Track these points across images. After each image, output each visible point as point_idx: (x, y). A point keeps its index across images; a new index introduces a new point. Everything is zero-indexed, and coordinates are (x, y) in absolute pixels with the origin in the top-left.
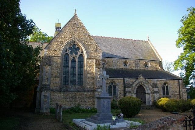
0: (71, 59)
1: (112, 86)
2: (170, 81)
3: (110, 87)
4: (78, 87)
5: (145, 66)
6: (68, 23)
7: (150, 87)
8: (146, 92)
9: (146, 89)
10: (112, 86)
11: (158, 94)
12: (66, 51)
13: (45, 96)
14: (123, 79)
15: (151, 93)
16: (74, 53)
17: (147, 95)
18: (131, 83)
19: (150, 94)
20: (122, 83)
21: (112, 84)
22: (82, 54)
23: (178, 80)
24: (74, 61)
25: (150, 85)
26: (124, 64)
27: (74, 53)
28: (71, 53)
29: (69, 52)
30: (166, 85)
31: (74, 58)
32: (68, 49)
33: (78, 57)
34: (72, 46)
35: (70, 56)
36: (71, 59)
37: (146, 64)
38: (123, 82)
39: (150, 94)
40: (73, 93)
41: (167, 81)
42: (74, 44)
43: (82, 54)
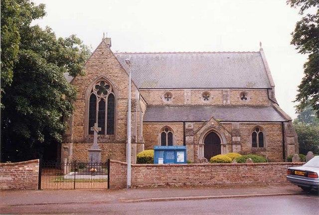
0: (98, 101)
1: (167, 133)
2: (226, 124)
3: (254, 135)
4: (107, 136)
5: (242, 99)
6: (152, 53)
7: (227, 134)
8: (222, 143)
9: (220, 137)
10: (167, 133)
11: (239, 146)
12: (92, 91)
13: (64, 148)
14: (183, 123)
15: (229, 144)
16: (102, 93)
17: (222, 147)
18: (195, 130)
19: (227, 146)
20: (182, 129)
21: (167, 131)
22: (112, 93)
23: (184, 122)
24: (102, 102)
25: (228, 132)
26: (204, 97)
27: (102, 93)
28: (99, 93)
29: (95, 92)
30: (260, 131)
31: (102, 99)
32: (94, 88)
33: (107, 97)
34: (99, 84)
35: (97, 98)
36: (98, 101)
37: (244, 96)
38: (182, 129)
39: (227, 146)
40: (101, 144)
41: (259, 124)
42: (102, 81)
43: (112, 93)
